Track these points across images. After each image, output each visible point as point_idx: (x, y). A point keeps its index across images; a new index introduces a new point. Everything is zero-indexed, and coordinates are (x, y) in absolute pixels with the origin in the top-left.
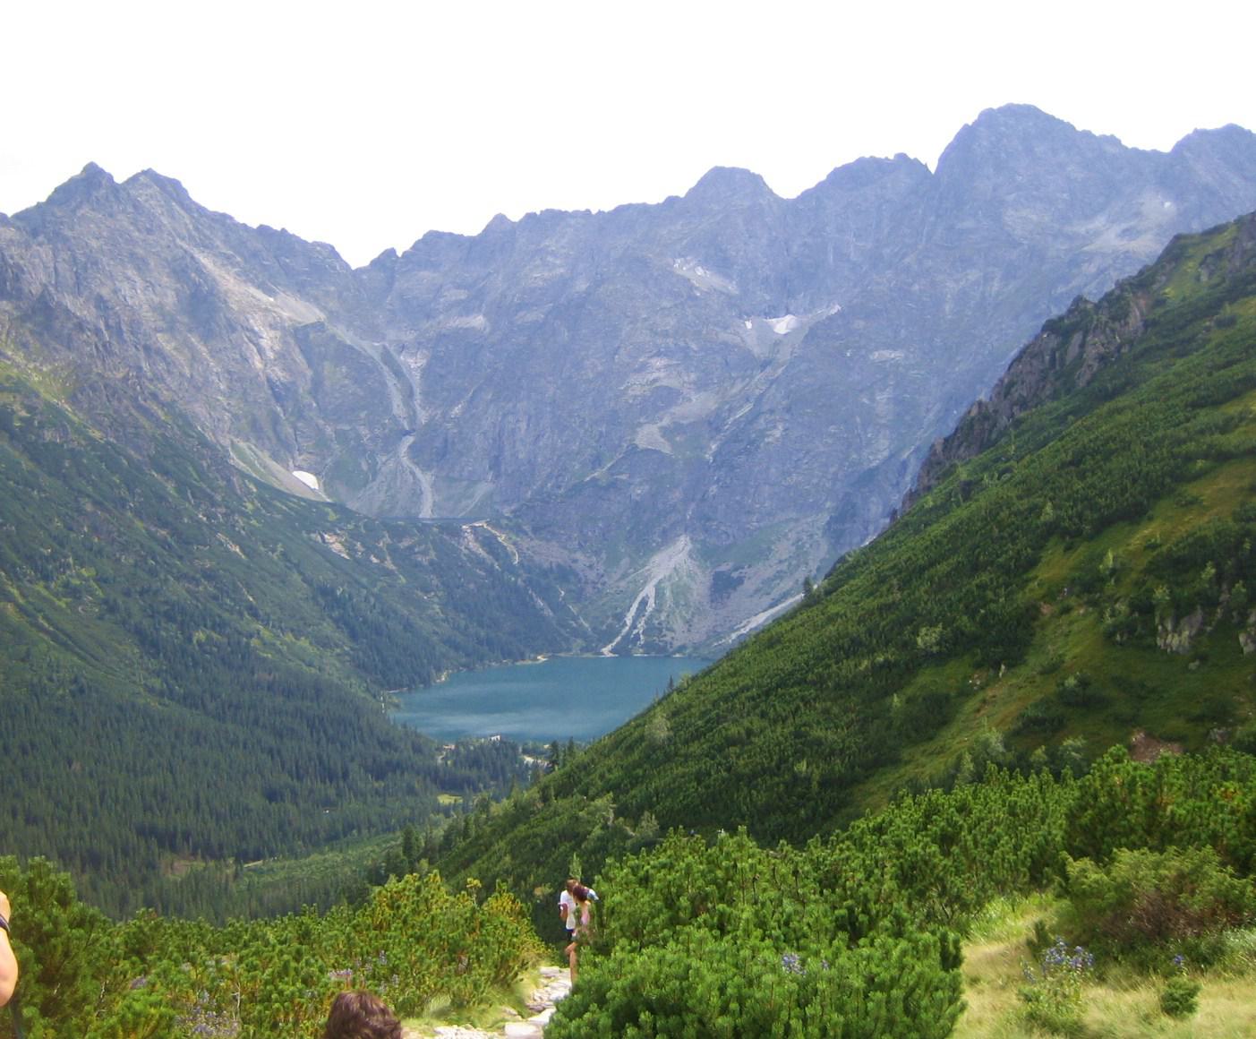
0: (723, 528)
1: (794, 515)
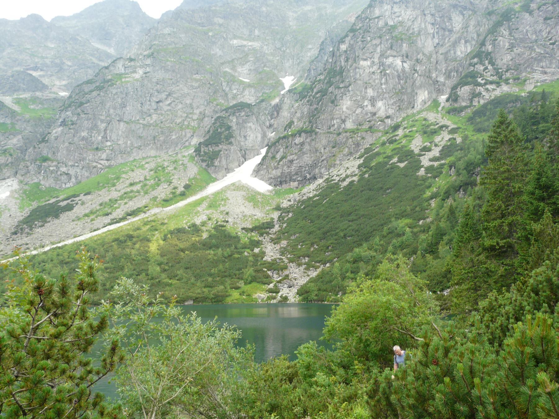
0: (64, 169)
1: (153, 153)
